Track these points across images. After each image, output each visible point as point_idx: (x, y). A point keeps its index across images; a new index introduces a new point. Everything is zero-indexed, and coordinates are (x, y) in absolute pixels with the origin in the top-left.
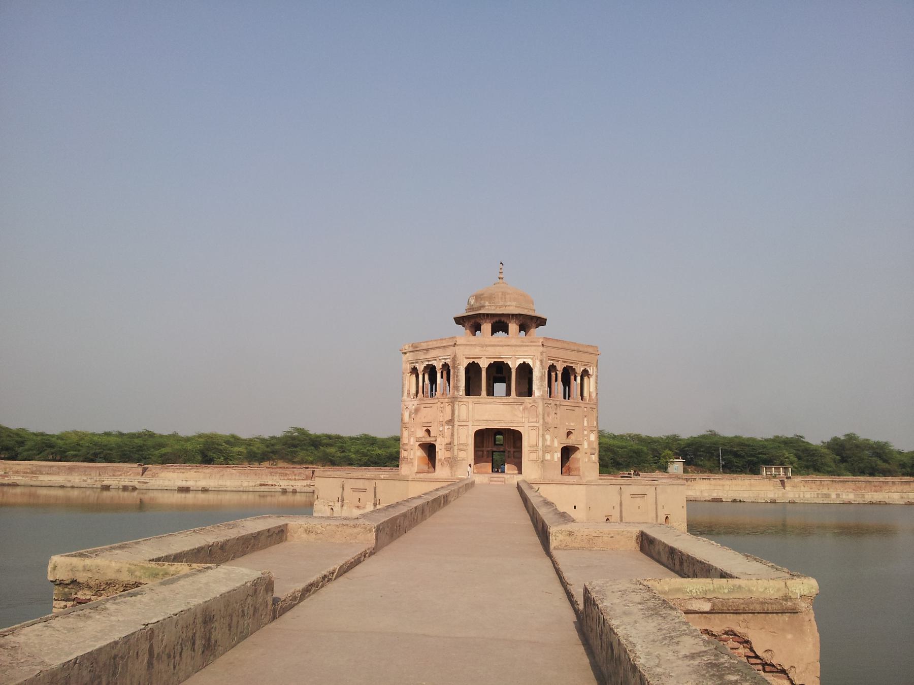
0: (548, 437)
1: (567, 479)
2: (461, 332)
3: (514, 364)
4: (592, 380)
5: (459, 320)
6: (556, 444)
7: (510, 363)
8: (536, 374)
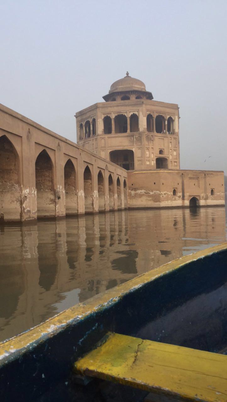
0: (147, 153)
3: (128, 115)
5: (105, 98)
7: (126, 115)
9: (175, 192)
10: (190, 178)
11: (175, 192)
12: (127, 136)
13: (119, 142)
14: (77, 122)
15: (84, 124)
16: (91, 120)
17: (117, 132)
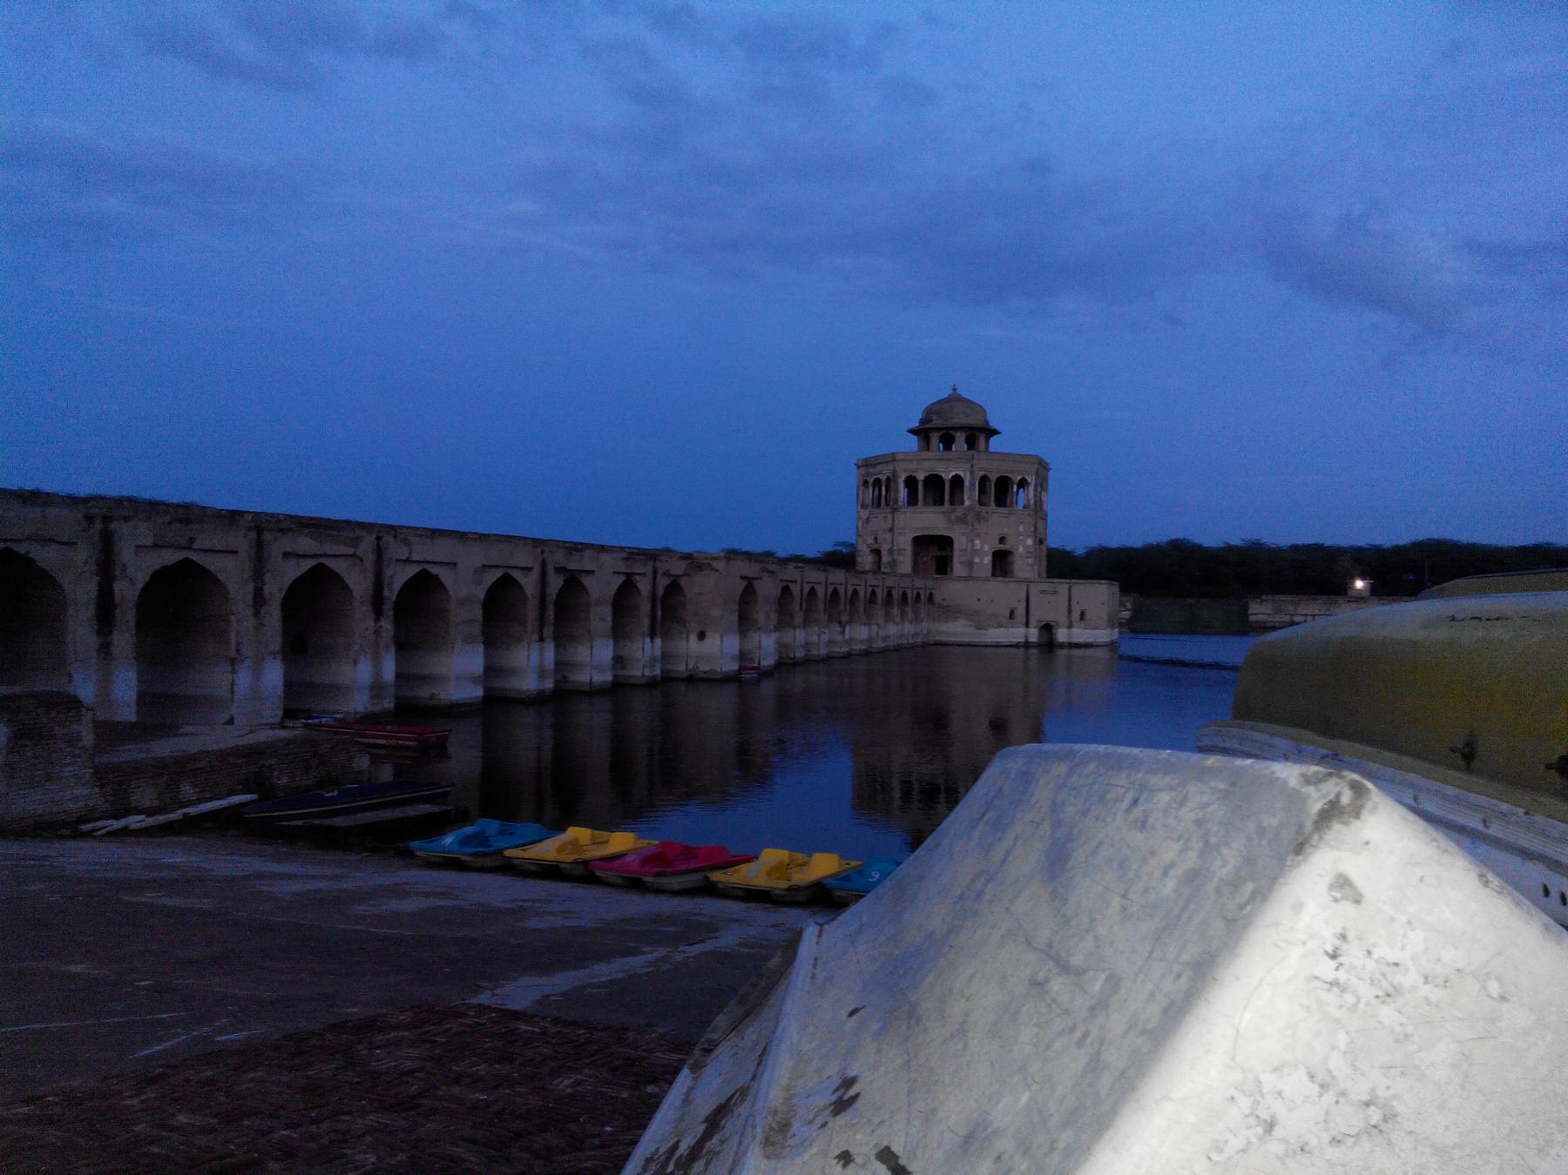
2: (913, 442)
3: (947, 476)
6: (986, 548)
8: (967, 484)
9: (1012, 614)
10: (1042, 592)
11: (1012, 614)
13: (929, 520)
16: (883, 478)
17: (926, 504)
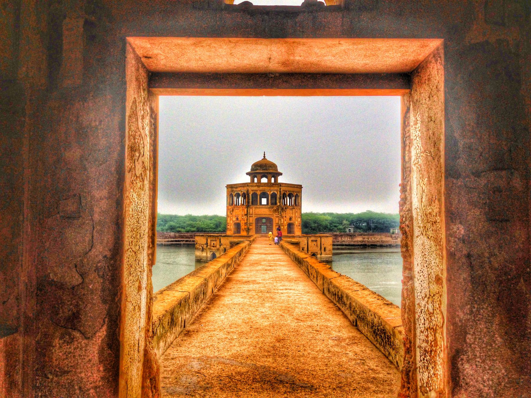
0: (282, 220)
1: (289, 235)
3: (270, 193)
4: (299, 198)
8: (278, 196)
12: (269, 208)
14: (227, 192)
15: (234, 194)
